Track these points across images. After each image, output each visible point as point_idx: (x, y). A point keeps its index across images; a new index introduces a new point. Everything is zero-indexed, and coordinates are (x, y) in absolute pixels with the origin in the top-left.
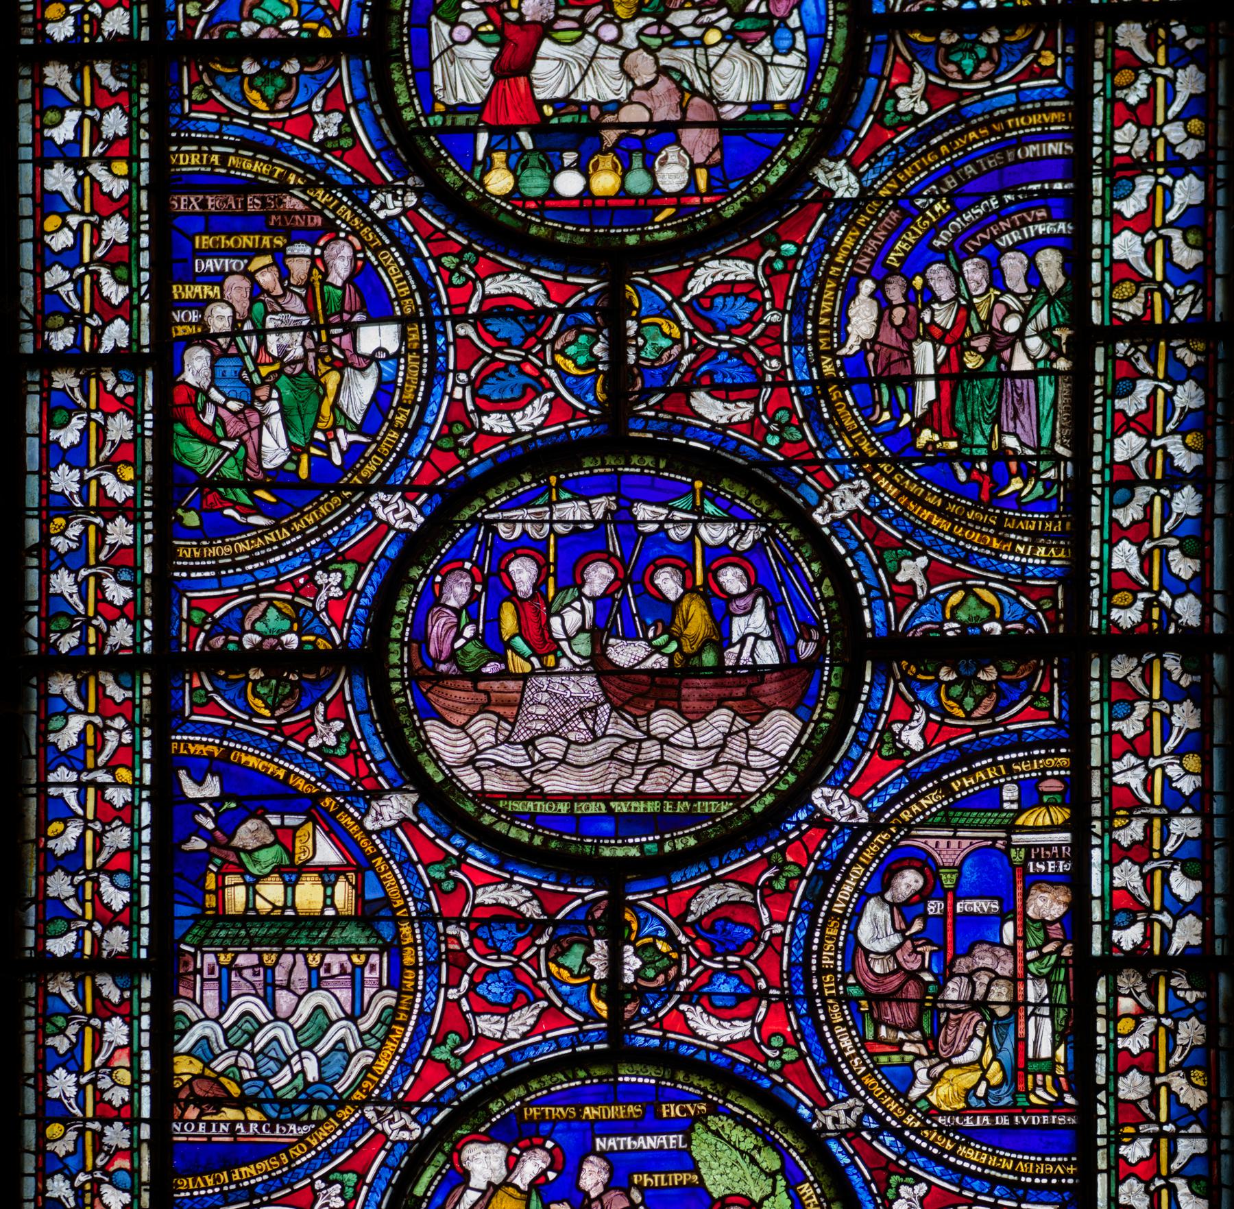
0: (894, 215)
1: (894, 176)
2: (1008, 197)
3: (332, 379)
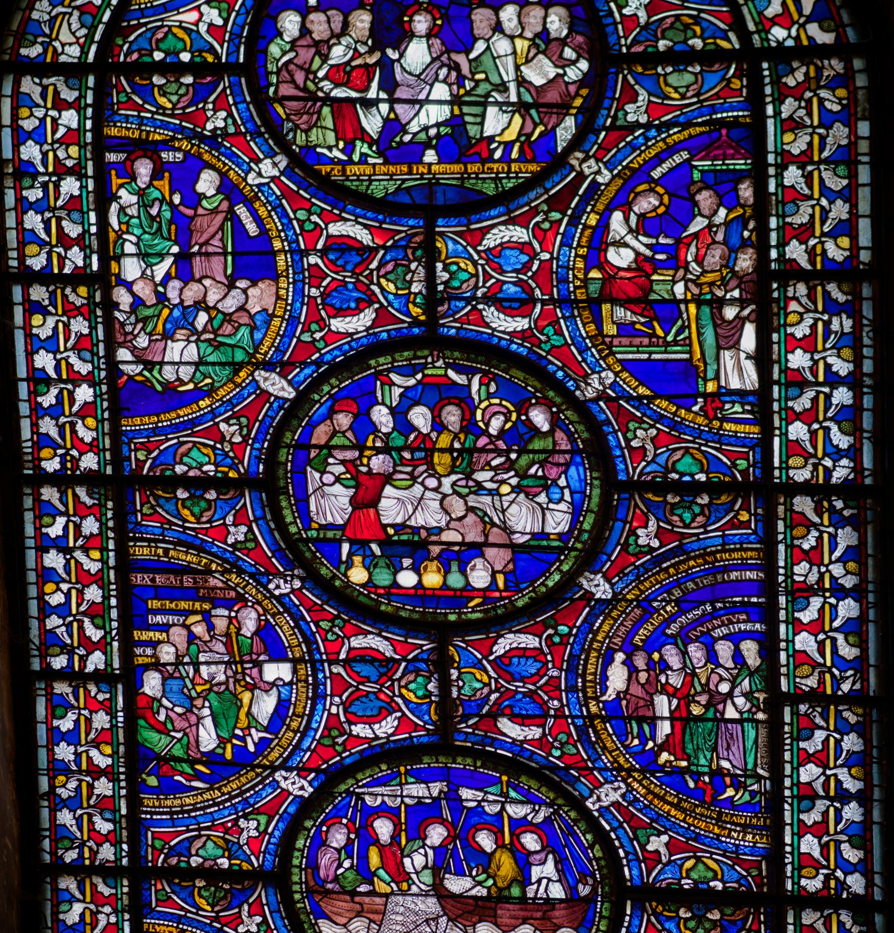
0: (638, 612)
1: (637, 586)
2: (719, 605)
3: (246, 697)
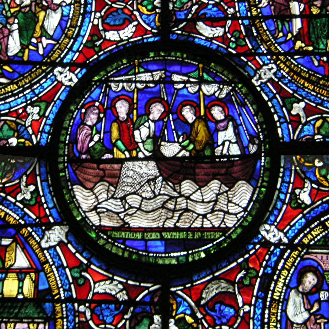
3: (42, 15)
